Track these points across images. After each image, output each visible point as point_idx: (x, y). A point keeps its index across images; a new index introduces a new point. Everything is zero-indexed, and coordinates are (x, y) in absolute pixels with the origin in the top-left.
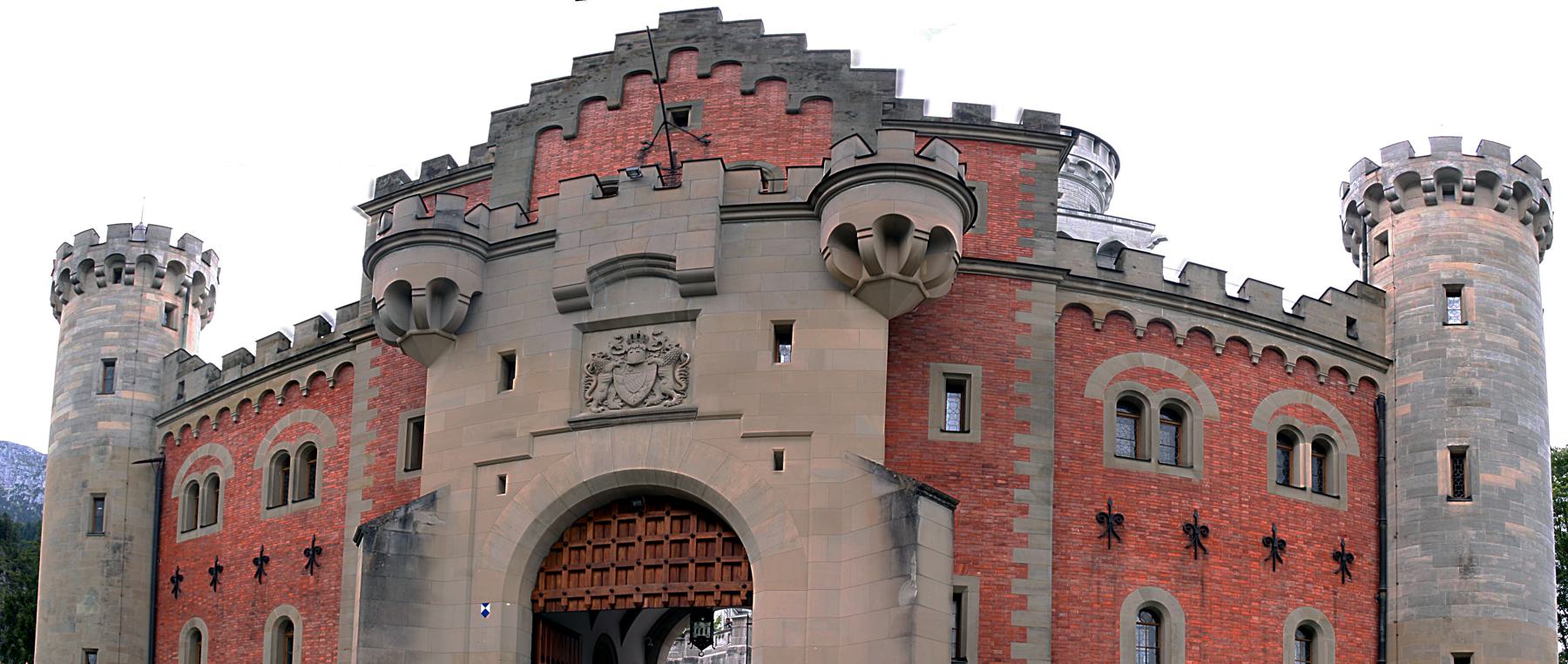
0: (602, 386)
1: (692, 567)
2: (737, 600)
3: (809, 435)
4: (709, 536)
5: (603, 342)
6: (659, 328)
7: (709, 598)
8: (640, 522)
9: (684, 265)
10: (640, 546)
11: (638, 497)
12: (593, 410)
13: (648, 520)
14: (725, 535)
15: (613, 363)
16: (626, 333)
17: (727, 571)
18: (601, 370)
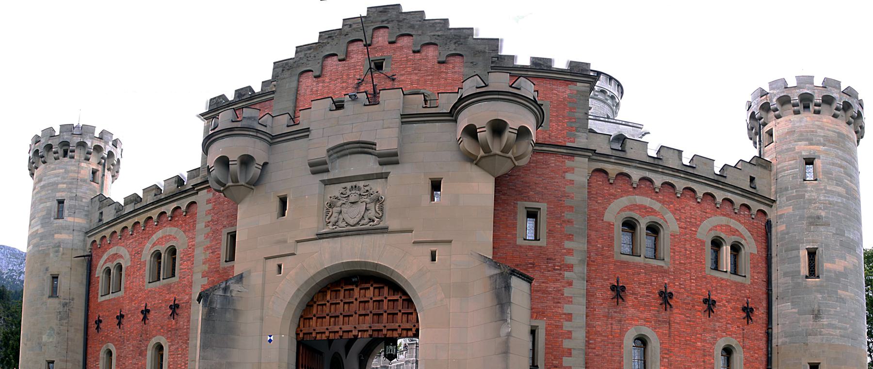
0: (335, 215)
1: (385, 315)
2: (410, 333)
3: (450, 242)
4: (395, 298)
5: (336, 190)
6: (367, 182)
7: (395, 332)
8: (357, 290)
9: (381, 147)
10: (356, 303)
11: (355, 276)
12: (330, 228)
13: (361, 289)
14: (403, 298)
15: (341, 202)
16: (349, 185)
17: (405, 317)
18: (335, 206)
